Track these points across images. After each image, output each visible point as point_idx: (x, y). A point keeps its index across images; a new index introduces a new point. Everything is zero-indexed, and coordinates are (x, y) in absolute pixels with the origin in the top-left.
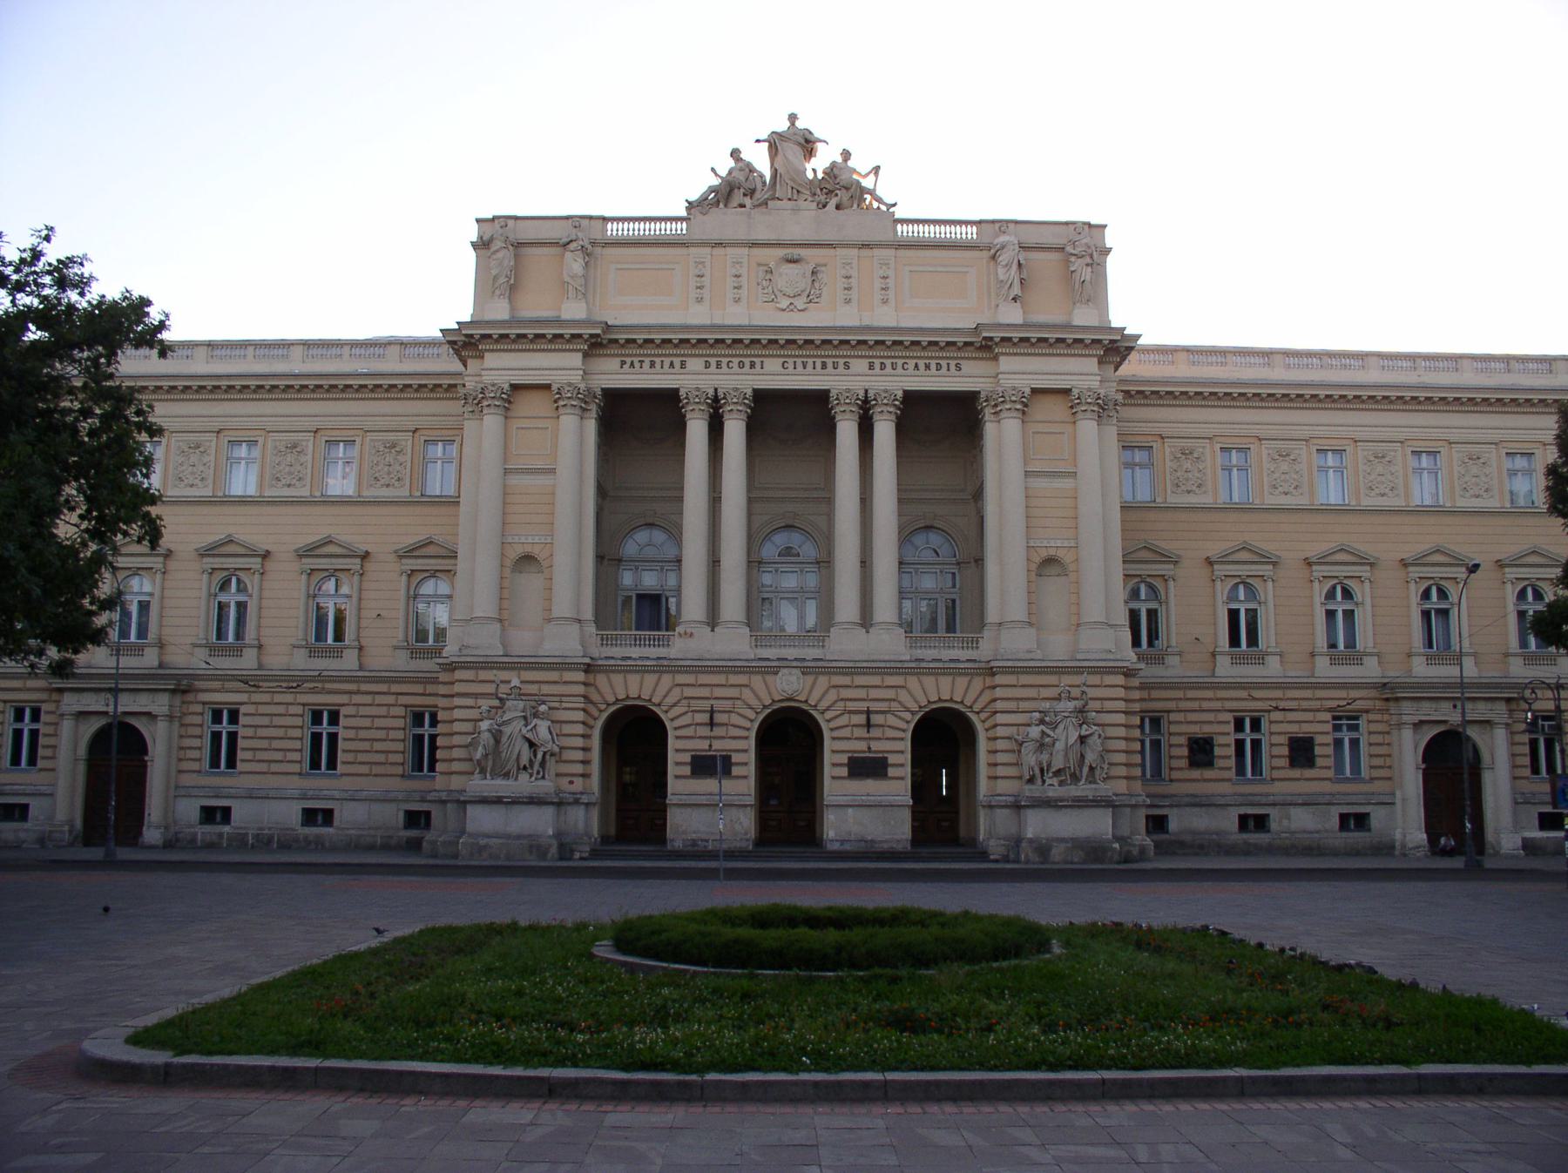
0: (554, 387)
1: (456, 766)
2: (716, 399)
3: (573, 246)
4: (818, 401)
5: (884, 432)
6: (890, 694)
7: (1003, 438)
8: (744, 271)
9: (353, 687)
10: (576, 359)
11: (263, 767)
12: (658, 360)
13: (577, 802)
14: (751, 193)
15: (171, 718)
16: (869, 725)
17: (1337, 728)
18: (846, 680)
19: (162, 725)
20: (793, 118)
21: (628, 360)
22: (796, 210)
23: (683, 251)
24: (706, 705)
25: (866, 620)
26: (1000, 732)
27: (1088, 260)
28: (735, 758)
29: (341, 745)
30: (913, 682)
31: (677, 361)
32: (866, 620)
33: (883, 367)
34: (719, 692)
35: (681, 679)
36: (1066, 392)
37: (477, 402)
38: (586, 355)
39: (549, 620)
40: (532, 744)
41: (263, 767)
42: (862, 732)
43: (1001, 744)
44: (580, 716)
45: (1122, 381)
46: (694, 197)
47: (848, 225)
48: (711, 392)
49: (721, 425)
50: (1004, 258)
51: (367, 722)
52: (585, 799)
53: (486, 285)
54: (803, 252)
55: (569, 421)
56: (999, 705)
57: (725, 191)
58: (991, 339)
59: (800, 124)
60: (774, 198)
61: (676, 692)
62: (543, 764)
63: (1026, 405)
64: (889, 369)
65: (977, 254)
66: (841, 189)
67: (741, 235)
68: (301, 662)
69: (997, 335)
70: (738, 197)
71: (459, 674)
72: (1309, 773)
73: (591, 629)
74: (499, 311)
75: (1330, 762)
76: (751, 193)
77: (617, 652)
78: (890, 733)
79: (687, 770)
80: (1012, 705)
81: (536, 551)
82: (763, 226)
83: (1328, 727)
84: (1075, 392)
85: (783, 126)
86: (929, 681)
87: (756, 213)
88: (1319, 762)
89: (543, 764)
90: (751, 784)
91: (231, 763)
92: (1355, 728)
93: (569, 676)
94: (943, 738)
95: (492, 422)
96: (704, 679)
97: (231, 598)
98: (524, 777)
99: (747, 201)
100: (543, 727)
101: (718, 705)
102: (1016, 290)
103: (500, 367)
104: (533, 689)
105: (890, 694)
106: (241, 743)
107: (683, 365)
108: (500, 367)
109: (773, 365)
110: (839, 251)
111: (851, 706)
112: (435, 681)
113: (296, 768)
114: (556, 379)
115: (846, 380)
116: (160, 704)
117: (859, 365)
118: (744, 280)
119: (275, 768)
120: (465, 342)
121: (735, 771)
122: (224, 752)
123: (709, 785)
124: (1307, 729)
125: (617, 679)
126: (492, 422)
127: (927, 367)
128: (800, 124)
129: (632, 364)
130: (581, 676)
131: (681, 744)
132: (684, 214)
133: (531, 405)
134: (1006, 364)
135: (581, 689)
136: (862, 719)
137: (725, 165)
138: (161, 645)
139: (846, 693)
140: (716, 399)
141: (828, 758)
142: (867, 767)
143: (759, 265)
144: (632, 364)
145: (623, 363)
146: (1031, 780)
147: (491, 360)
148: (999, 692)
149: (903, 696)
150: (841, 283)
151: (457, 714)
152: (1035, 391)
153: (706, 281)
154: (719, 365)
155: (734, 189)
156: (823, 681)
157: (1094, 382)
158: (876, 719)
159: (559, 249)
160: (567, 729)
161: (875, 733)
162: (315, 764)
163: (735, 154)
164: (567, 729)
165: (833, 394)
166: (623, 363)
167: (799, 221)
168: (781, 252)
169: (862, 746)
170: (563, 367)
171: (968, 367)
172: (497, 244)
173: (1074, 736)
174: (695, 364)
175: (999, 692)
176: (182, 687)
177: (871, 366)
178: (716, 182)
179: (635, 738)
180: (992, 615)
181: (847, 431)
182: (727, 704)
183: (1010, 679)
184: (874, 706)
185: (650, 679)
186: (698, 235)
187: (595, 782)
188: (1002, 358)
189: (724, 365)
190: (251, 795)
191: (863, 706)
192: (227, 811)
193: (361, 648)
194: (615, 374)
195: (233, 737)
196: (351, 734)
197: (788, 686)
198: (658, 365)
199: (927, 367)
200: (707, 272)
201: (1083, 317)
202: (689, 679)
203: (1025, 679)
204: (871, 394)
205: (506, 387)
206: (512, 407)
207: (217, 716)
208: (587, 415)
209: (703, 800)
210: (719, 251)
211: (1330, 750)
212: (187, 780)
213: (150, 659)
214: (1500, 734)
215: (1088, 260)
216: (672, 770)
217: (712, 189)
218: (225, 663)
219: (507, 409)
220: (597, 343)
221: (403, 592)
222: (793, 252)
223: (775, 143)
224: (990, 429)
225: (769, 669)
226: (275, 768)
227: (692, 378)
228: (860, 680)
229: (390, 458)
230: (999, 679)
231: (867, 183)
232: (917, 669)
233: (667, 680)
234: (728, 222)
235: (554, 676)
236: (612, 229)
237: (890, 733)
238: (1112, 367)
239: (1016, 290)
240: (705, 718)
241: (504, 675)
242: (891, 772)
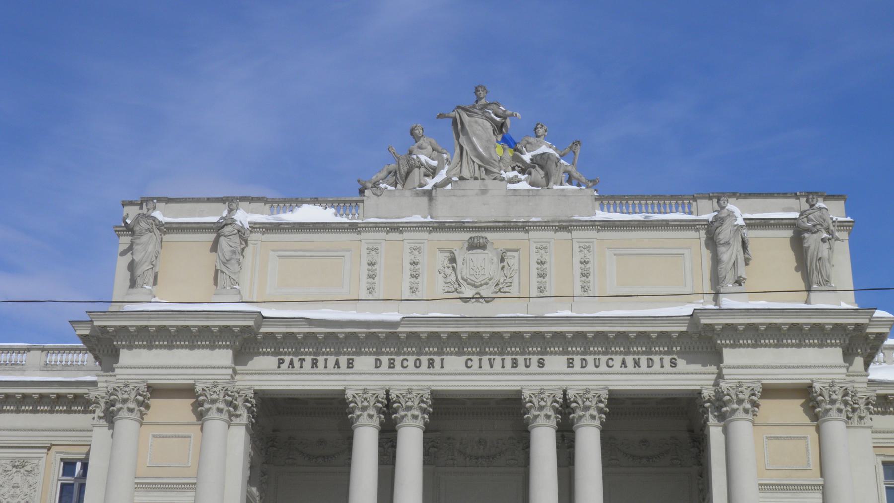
0: (199, 388)
3: (227, 230)
4: (511, 410)
5: (589, 441)
10: (224, 356)
12: (321, 359)
21: (287, 359)
22: (484, 191)
23: (353, 236)
27: (825, 235)
31: (343, 360)
45: (872, 383)
48: (382, 395)
49: (394, 432)
50: (724, 233)
54: (490, 235)
58: (710, 327)
63: (755, 404)
64: (590, 367)
65: (692, 234)
69: (720, 321)
84: (817, 387)
107: (350, 364)
109: (454, 362)
114: (201, 380)
115: (540, 379)
117: (556, 362)
127: (637, 363)
129: (291, 363)
143: (442, 251)
144: (291, 363)
145: (281, 362)
150: (534, 272)
153: (380, 269)
154: (392, 365)
157: (839, 375)
165: (526, 394)
166: (281, 362)
168: (466, 236)
170: (210, 365)
172: (143, 225)
174: (365, 362)
177: (570, 364)
188: (726, 352)
189: (398, 363)
194: (269, 375)
198: (321, 363)
199: (637, 363)
204: (571, 394)
205: (143, 387)
206: (149, 412)
208: (238, 420)
210: (395, 236)
215: (825, 235)
219: (142, 415)
222: (477, 235)
224: (715, 433)
227: (359, 378)
229: (18, 478)
238: (859, 361)
239: (742, 271)
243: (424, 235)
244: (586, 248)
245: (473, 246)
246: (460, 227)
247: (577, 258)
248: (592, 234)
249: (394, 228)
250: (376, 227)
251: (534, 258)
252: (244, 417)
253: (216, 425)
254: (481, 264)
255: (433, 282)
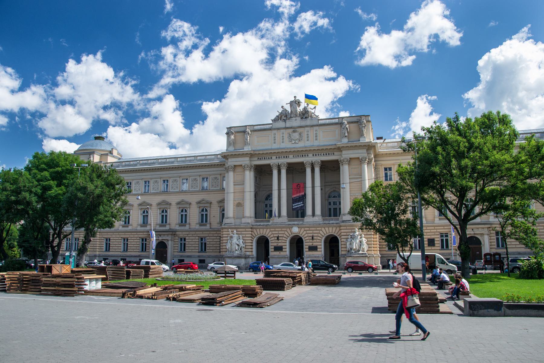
1: (224, 250)
2: (279, 166)
5: (317, 170)
6: (318, 232)
7: (345, 170)
8: (284, 135)
9: (209, 233)
10: (248, 159)
11: (190, 251)
13: (249, 257)
14: (286, 116)
15: (172, 240)
16: (313, 239)
17: (442, 236)
18: (308, 229)
19: (170, 242)
20: (295, 97)
22: (296, 120)
24: (277, 235)
25: (314, 215)
26: (342, 240)
28: (284, 247)
29: (207, 245)
30: (323, 229)
32: (314, 215)
33: (316, 155)
34: (280, 232)
35: (272, 230)
36: (359, 158)
37: (227, 170)
38: (250, 157)
39: (244, 217)
40: (238, 245)
41: (190, 251)
42: (311, 241)
43: (342, 243)
44: (251, 238)
46: (273, 119)
47: (308, 122)
51: (212, 240)
52: (251, 256)
53: (229, 144)
54: (297, 129)
55: (247, 173)
56: (342, 234)
57: (280, 117)
59: (297, 98)
60: (291, 117)
61: (271, 233)
62: (241, 249)
66: (305, 114)
67: (284, 126)
68: (198, 227)
70: (283, 118)
71: (224, 230)
72: (433, 248)
73: (253, 219)
74: (232, 149)
75: (440, 245)
76: (286, 116)
77: (258, 224)
78: (318, 241)
79: (273, 250)
80: (345, 234)
81: (241, 202)
82: (289, 124)
83: (439, 236)
84: (360, 158)
85: (293, 99)
86: (327, 229)
87: (287, 121)
88: (436, 245)
89: (241, 249)
90: (288, 253)
91: (184, 250)
92: (447, 236)
93: (247, 230)
94: (332, 243)
95: (231, 174)
96: (276, 230)
97: (184, 213)
98: (237, 252)
99: (285, 118)
100: (241, 241)
101: (280, 235)
102: (346, 134)
103: (231, 162)
104: (240, 233)
105: (318, 232)
106: (186, 245)
108: (231, 162)
109: (291, 156)
110: (307, 129)
111: (309, 235)
112: (220, 231)
113: (197, 251)
116: (169, 238)
118: (285, 138)
119: (193, 251)
120: (225, 156)
121: (284, 250)
122: (183, 247)
123: (277, 253)
124: (433, 237)
125: (258, 230)
126: (231, 174)
128: (297, 98)
130: (250, 230)
131: (272, 244)
132: (271, 122)
133: (239, 170)
134: (344, 152)
135: (250, 233)
136: (311, 238)
137: (280, 110)
138: (169, 224)
139: (308, 232)
140: (279, 166)
141: (304, 247)
142: (313, 248)
146: (349, 251)
147: (230, 160)
148: (342, 231)
149: (321, 232)
151: (224, 238)
152: (350, 158)
155: (284, 116)
156: (303, 229)
158: (315, 238)
159: (243, 134)
160: (247, 241)
161: (314, 241)
162: (202, 250)
163: (282, 107)
164: (247, 241)
167: (296, 122)
168: (292, 130)
169: (311, 244)
170: (245, 161)
171: (335, 153)
173: (358, 241)
174: (274, 157)
175: (342, 231)
176: (173, 232)
178: (278, 114)
179: (263, 243)
180: (342, 212)
181: (308, 171)
182: (282, 235)
183: (345, 228)
184: (314, 235)
185: (265, 230)
186: (274, 127)
187: (254, 253)
190: (188, 256)
191: (312, 235)
192: (183, 261)
193: (210, 224)
195: (185, 244)
196: (208, 243)
197: (295, 230)
200: (276, 136)
201: (362, 140)
202: (273, 230)
203: (348, 228)
207: (181, 239)
209: (276, 256)
210: (279, 131)
211: (440, 242)
212: (176, 254)
213: (167, 228)
214: (486, 238)
216: (270, 250)
217: (277, 116)
218: (183, 228)
220: (251, 155)
221: (219, 211)
222: (294, 129)
223: (291, 103)
224: (341, 167)
225: (291, 227)
226: (193, 251)
227: (273, 161)
228: (311, 229)
229: (215, 181)
230: (342, 228)
231: (313, 111)
232: (325, 225)
233: (268, 230)
234: (281, 124)
235: (244, 230)
236: (256, 127)
237: (318, 241)
240: (276, 238)
241: (232, 230)
242: (318, 250)
243: (284, 131)
244: (316, 131)
245: (294, 132)
246: (291, 128)
247: (315, 133)
248: (317, 128)
249: (279, 129)
250: (275, 129)
251: (306, 133)
252: (252, 169)
253: (247, 173)
254: (296, 135)
255: (286, 139)
